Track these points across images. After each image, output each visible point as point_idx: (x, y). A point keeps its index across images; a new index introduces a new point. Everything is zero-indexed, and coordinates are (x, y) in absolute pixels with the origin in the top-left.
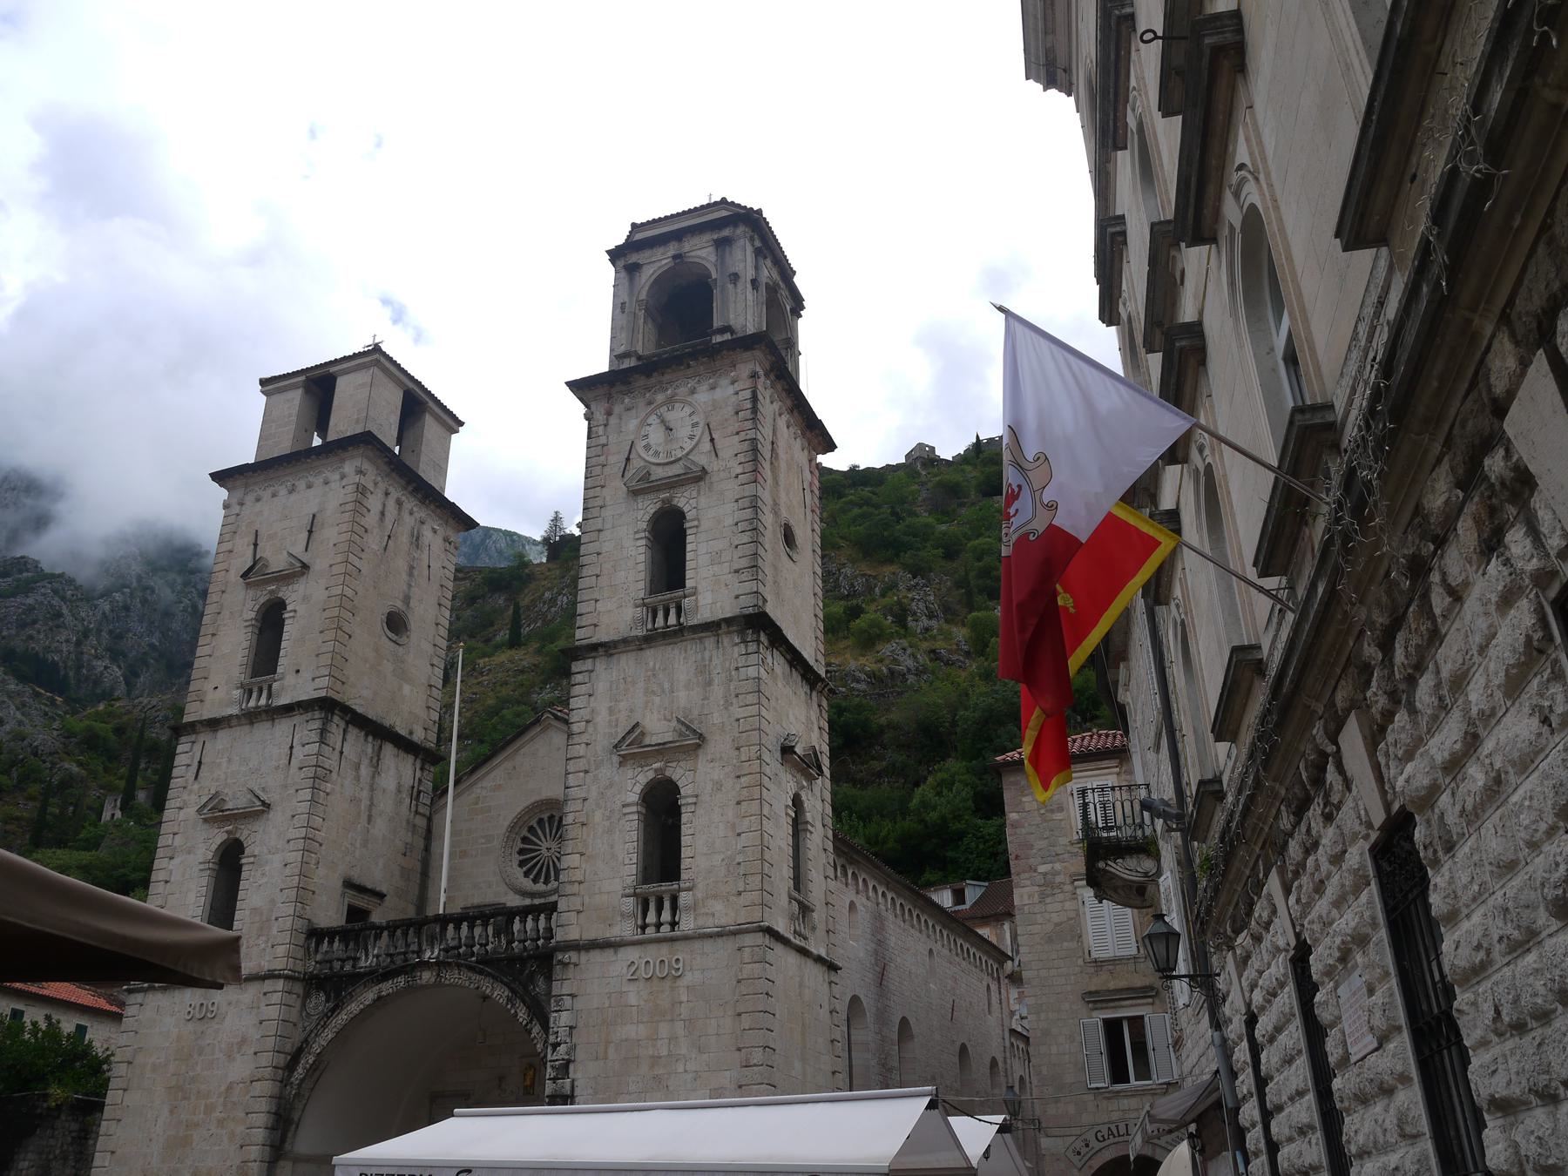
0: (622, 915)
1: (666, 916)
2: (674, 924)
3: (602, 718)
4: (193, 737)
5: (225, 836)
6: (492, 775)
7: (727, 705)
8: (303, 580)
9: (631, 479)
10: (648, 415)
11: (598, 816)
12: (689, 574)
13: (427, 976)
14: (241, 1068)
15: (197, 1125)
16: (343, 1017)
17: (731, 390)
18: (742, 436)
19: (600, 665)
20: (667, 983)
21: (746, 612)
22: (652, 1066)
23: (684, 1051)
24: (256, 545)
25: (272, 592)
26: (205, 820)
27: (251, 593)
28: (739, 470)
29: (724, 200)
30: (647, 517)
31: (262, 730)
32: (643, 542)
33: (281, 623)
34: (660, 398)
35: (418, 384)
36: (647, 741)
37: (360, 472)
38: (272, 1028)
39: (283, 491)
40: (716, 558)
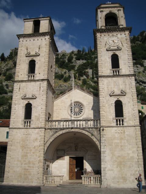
1: (121, 123)
2: (123, 124)
6: (65, 96)
7: (130, 89)
8: (38, 57)
9: (108, 48)
11: (107, 105)
12: (120, 66)
14: (37, 144)
15: (28, 153)
17: (125, 36)
22: (121, 147)
26: (22, 99)
28: (128, 50)
30: (111, 55)
31: (33, 83)
32: (111, 59)
34: (111, 35)
37: (49, 39)
40: (125, 64)
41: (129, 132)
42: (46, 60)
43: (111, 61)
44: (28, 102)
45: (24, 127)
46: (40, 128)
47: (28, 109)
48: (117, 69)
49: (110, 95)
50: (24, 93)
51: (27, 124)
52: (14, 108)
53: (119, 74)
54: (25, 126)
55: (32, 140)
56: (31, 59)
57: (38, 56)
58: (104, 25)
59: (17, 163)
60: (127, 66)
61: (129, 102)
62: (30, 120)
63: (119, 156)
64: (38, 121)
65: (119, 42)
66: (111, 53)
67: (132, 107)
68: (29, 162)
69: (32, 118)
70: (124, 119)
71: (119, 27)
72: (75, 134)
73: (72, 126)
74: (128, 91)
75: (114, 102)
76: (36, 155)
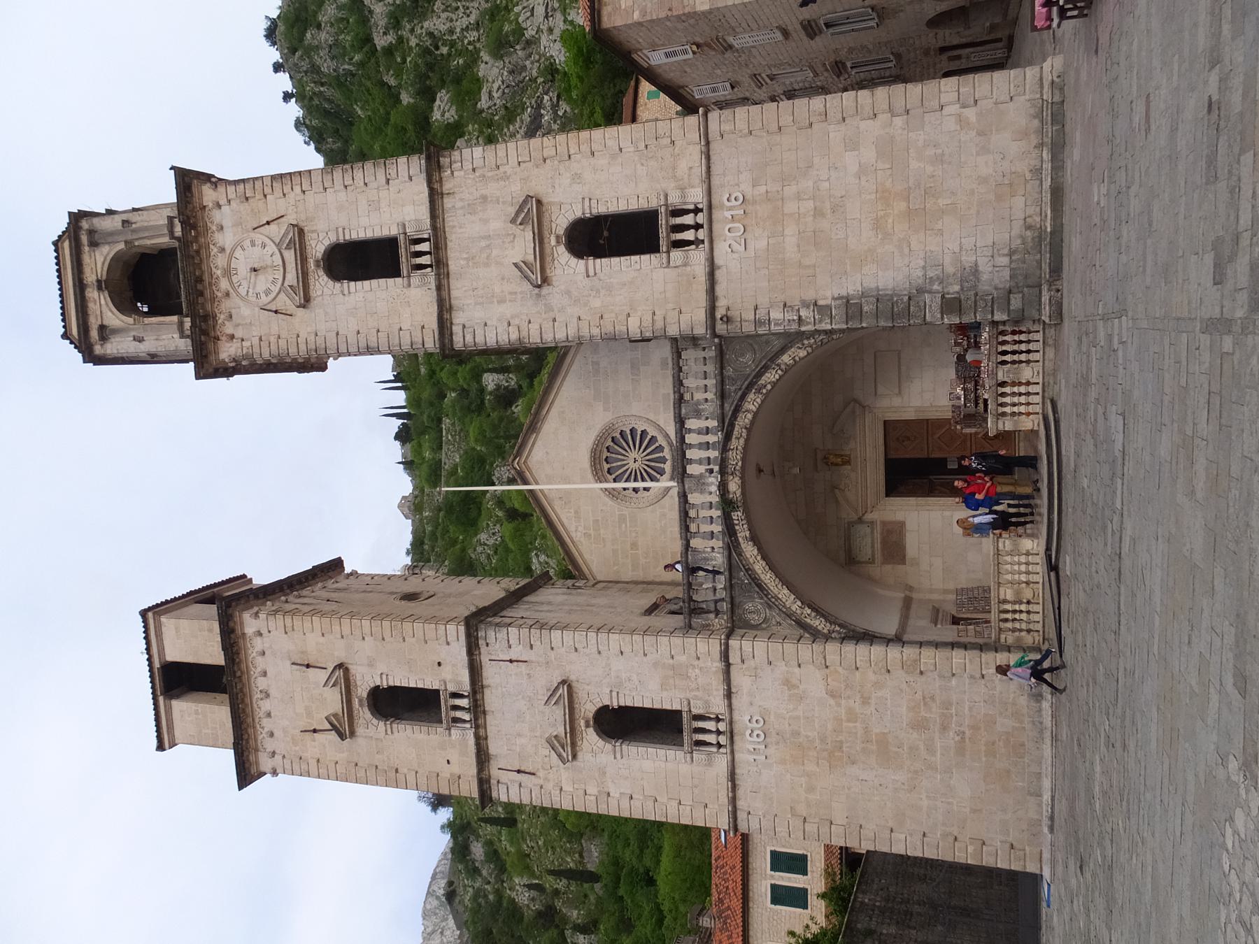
0: (685, 265)
1: (688, 219)
2: (697, 211)
3: (507, 310)
4: (493, 782)
5: (591, 730)
7: (506, 177)
8: (353, 669)
10: (238, 294)
11: (596, 303)
13: (734, 486)
14: (813, 682)
15: (867, 730)
16: (767, 578)
17: (225, 209)
18: (268, 190)
19: (459, 318)
20: (750, 208)
21: (423, 168)
22: (823, 215)
23: (810, 184)
24: (315, 731)
25: (361, 705)
26: (574, 757)
27: (360, 730)
28: (297, 189)
29: (55, 244)
30: (331, 283)
31: (491, 700)
33: (394, 690)
34: (224, 284)
35: (191, 593)
36: (530, 258)
37: (256, 615)
38: (776, 647)
39: (266, 705)
40: (374, 205)
41: (740, 172)
42: (367, 629)
43: (359, 283)
44: (587, 726)
45: (722, 750)
46: (728, 665)
47: (623, 724)
48: (402, 251)
49: (539, 287)
50: (546, 751)
51: (709, 731)
52: (625, 803)
53: (428, 240)
54: (719, 746)
55: (795, 709)
56: (366, 710)
57: (347, 670)
58: (175, 318)
59: (923, 796)
60: (383, 194)
61: (577, 178)
62: (684, 715)
63: (878, 225)
64: (693, 673)
65: (259, 237)
66: (322, 284)
67: (601, 161)
68: (920, 725)
69: (676, 707)
70: (666, 205)
71: (178, 239)
72: (760, 471)
73: (714, 488)
74: (516, 190)
75: (578, 265)
76: (878, 685)
